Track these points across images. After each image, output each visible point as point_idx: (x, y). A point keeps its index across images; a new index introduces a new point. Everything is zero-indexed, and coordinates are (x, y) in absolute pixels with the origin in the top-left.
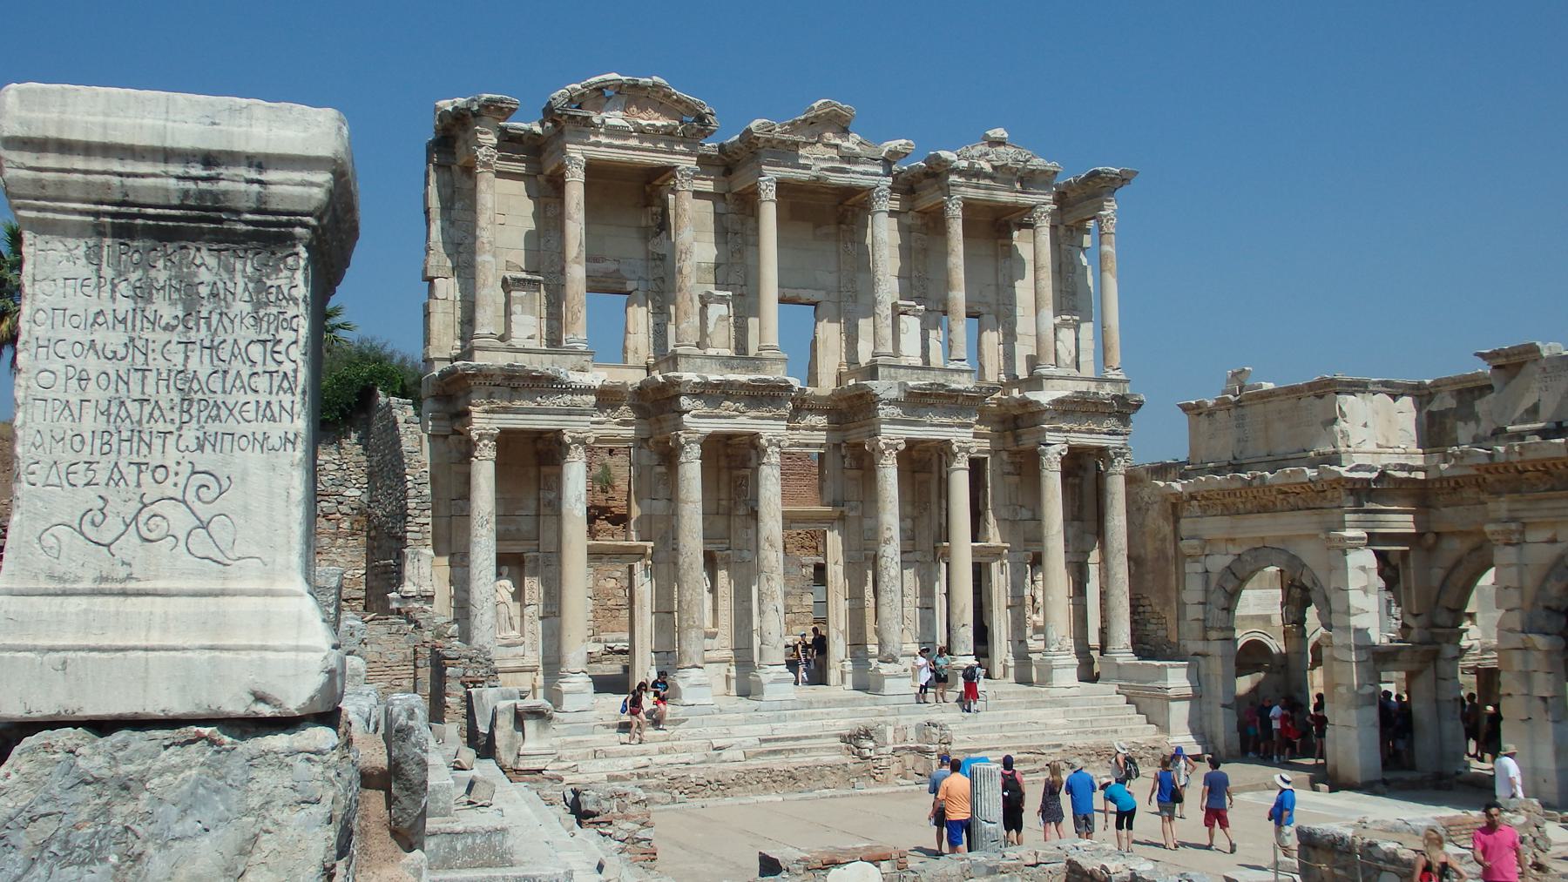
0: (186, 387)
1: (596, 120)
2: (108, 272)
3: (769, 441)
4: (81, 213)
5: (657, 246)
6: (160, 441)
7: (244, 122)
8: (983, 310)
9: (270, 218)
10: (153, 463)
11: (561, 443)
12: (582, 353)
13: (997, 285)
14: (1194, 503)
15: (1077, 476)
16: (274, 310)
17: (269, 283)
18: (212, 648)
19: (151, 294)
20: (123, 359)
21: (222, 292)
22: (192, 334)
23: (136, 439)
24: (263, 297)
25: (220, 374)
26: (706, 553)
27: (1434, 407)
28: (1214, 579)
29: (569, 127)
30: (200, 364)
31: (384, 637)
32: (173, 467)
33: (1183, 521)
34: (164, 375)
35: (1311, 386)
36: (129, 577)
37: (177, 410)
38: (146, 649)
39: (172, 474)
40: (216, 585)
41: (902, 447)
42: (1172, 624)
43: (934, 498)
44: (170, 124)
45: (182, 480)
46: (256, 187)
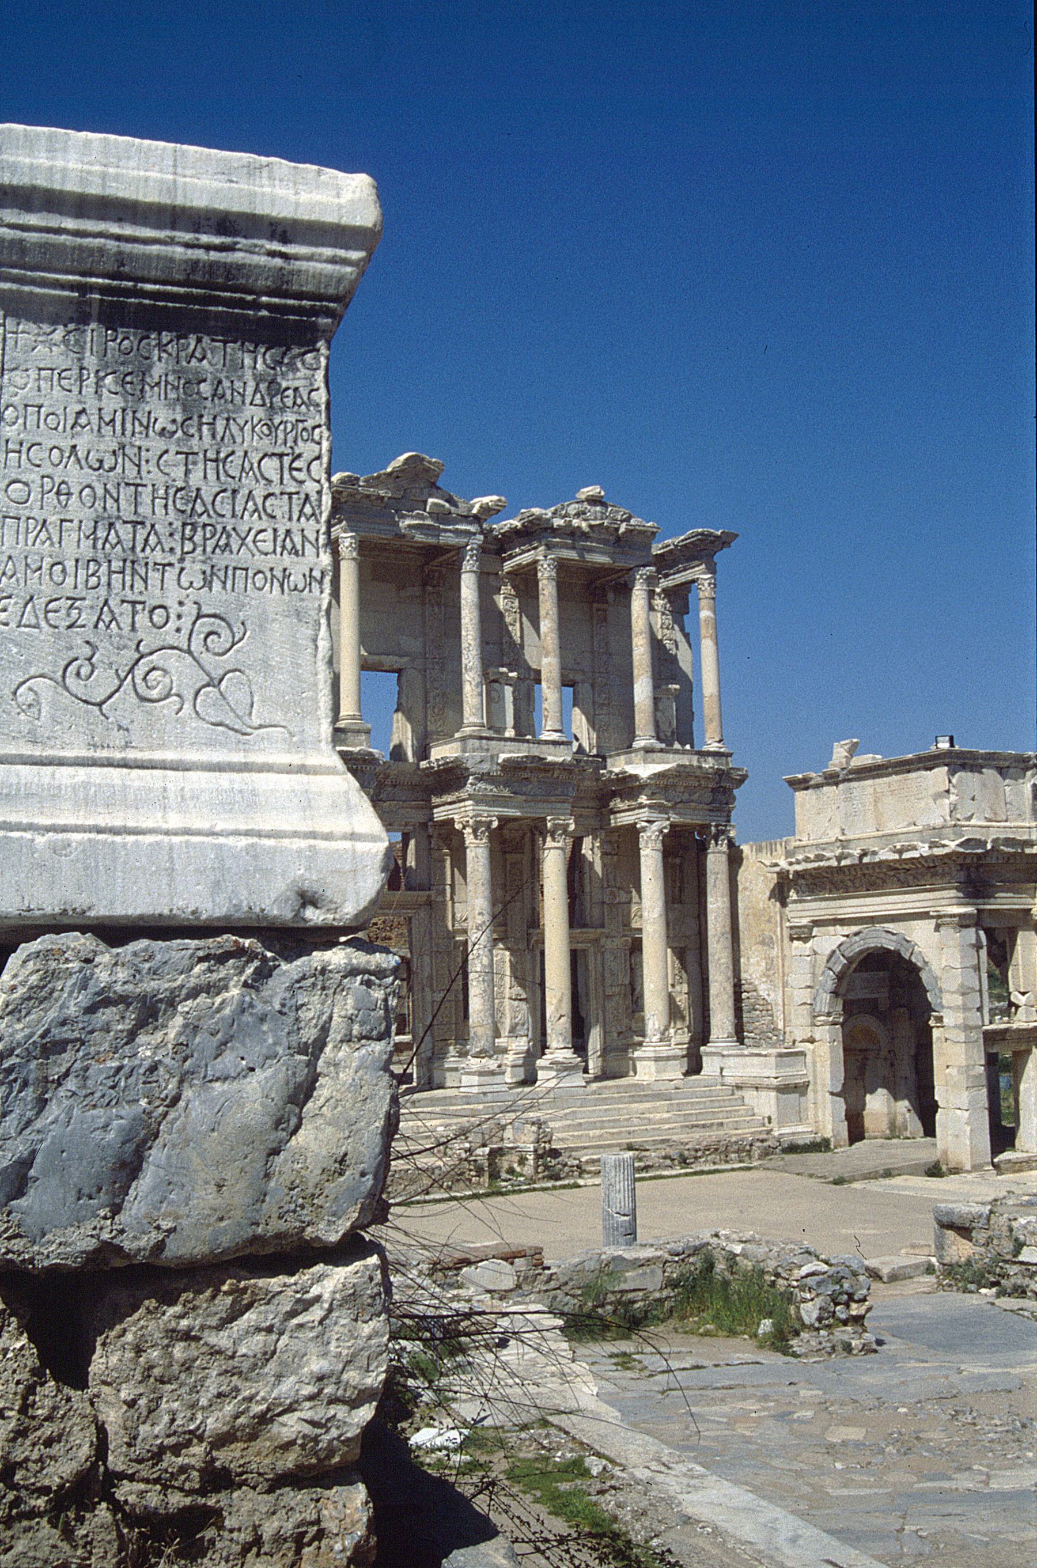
0: (189, 508)
2: (91, 361)
4: (62, 286)
6: (158, 575)
7: (265, 181)
9: (291, 302)
10: (152, 602)
13: (592, 652)
16: (291, 417)
17: (284, 385)
18: (247, 833)
19: (142, 390)
20: (112, 469)
21: (228, 392)
22: (195, 441)
23: (128, 571)
24: (277, 399)
25: (228, 494)
28: (822, 960)
30: (202, 479)
32: (174, 609)
34: (161, 492)
36: (127, 745)
37: (177, 536)
38: (167, 833)
39: (173, 617)
40: (238, 757)
41: (495, 824)
44: (181, 180)
45: (186, 623)
46: (278, 262)
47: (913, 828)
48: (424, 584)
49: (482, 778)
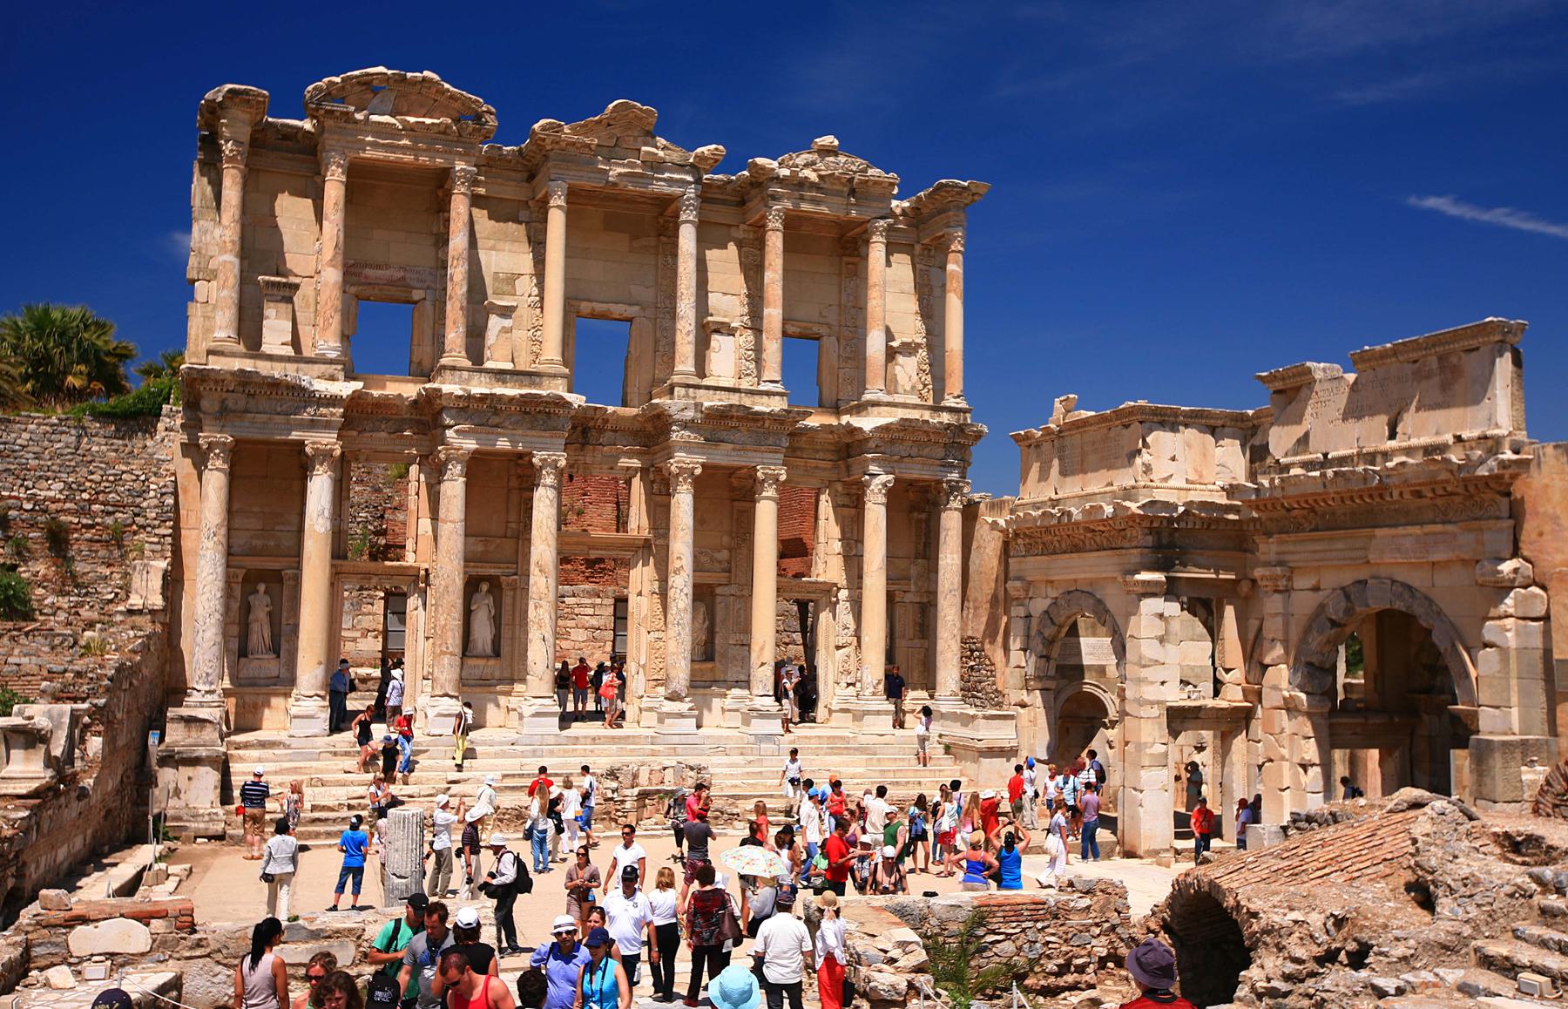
1: (359, 116)
8: (823, 330)
12: (331, 362)
41: (698, 471)
49: (685, 425)
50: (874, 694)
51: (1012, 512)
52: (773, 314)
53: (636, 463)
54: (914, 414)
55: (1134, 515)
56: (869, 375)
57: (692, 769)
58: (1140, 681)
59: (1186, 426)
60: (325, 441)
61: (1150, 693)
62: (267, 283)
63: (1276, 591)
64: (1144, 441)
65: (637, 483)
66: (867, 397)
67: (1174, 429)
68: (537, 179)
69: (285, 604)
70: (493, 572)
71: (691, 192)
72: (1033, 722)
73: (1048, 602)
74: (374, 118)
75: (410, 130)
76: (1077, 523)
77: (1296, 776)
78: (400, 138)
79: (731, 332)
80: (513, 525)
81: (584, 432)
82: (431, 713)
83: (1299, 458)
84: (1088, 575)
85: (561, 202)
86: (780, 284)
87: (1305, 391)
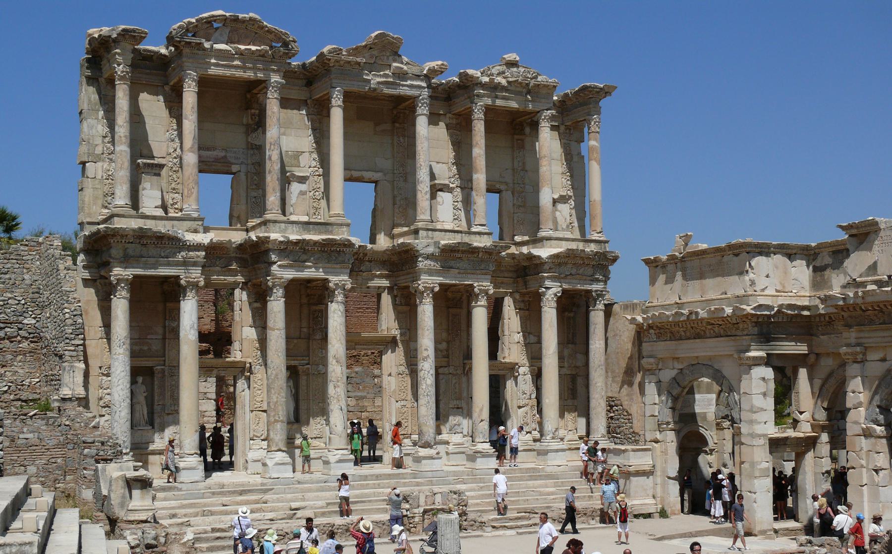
3: (336, 285)
5: (253, 139)
8: (502, 187)
11: (179, 285)
12: (195, 219)
13: (513, 170)
14: (652, 331)
15: (572, 311)
26: (289, 368)
27: (818, 263)
29: (186, 51)
31: (44, 428)
33: (643, 344)
35: (730, 247)
41: (437, 289)
42: (635, 422)
43: (464, 327)
47: (723, 296)
48: (394, 122)
49: (429, 257)
50: (553, 438)
51: (644, 312)
52: (480, 178)
53: (385, 283)
54: (573, 246)
55: (748, 314)
56: (542, 218)
57: (455, 493)
58: (751, 422)
59: (775, 254)
60: (193, 276)
61: (759, 429)
62: (145, 164)
63: (855, 362)
64: (750, 264)
65: (386, 299)
66: (542, 234)
67: (767, 255)
68: (315, 85)
69: (157, 390)
70: (293, 363)
71: (425, 93)
72: (665, 452)
73: (675, 372)
74: (217, 46)
75: (241, 53)
76: (702, 319)
77: (872, 477)
78: (234, 59)
79: (450, 190)
80: (305, 330)
81: (359, 262)
82: (270, 463)
83: (870, 278)
84: (709, 354)
85: (340, 103)
86: (484, 157)
87: (873, 236)
